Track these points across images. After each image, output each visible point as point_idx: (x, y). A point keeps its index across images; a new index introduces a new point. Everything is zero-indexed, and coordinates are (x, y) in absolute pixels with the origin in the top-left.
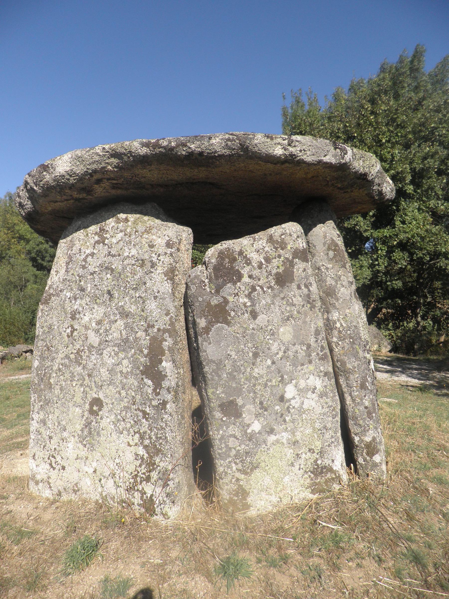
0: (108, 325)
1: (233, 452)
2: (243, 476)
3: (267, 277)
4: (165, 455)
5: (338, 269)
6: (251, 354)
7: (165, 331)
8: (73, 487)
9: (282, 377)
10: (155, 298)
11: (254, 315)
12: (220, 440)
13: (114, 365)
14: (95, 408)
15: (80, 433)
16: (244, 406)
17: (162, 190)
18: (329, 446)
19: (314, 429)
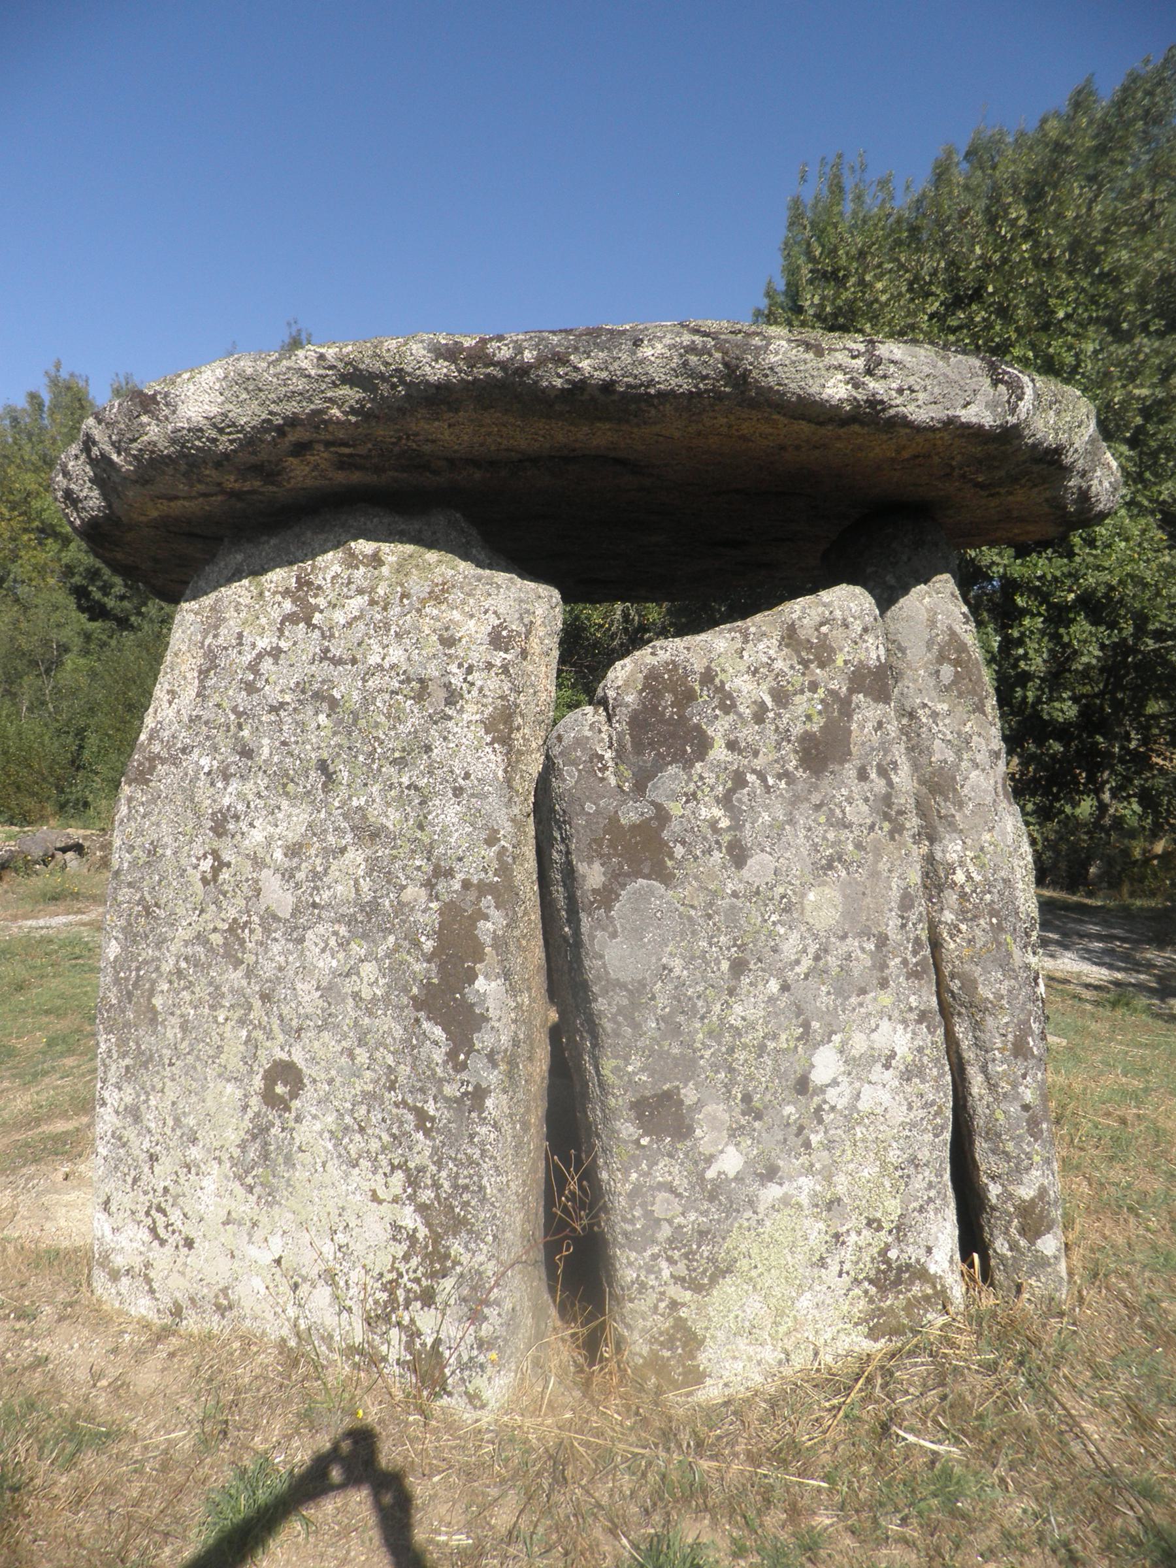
0: (318, 861)
1: (666, 1231)
2: (688, 1295)
3: (778, 747)
4: (478, 1237)
5: (965, 717)
6: (725, 965)
7: (484, 888)
8: (217, 1296)
9: (806, 1025)
10: (458, 792)
11: (738, 855)
12: (633, 1194)
13: (335, 973)
14: (280, 1089)
15: (236, 1152)
16: (699, 1105)
17: (478, 475)
18: (921, 1210)
19: (884, 1165)
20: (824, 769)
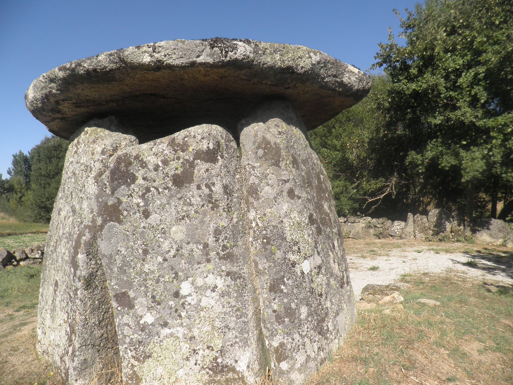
1: (127, 340)
2: (136, 363)
3: (164, 179)
5: (267, 167)
6: (141, 251)
9: (176, 274)
11: (146, 214)
16: (135, 298)
17: (114, 104)
18: (232, 345)
19: (213, 327)
20: (182, 185)
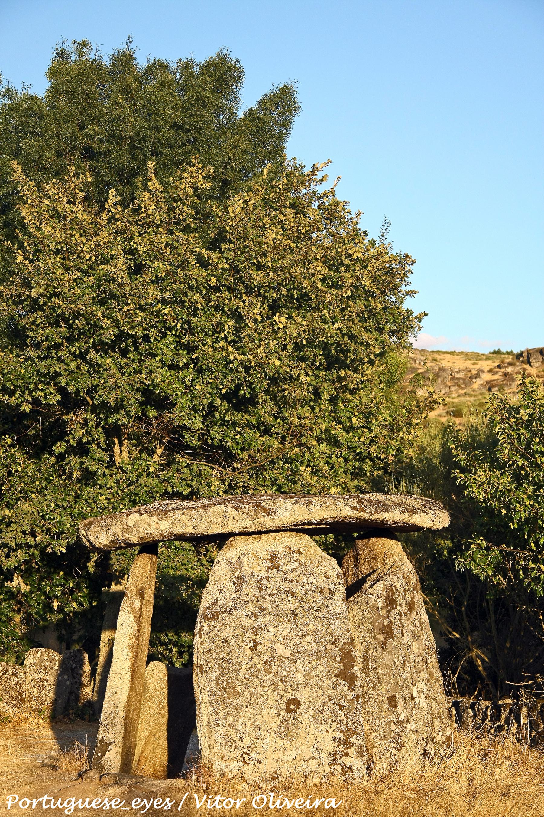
10: (338, 618)
14: (292, 707)
15: (276, 729)
